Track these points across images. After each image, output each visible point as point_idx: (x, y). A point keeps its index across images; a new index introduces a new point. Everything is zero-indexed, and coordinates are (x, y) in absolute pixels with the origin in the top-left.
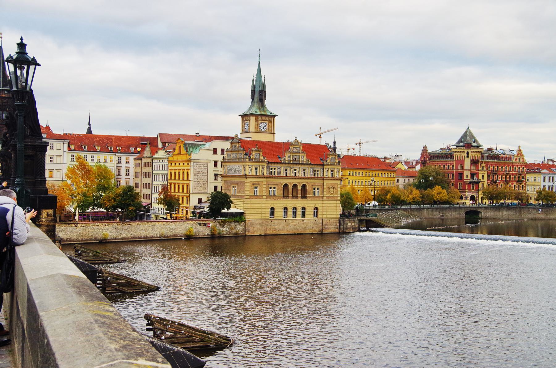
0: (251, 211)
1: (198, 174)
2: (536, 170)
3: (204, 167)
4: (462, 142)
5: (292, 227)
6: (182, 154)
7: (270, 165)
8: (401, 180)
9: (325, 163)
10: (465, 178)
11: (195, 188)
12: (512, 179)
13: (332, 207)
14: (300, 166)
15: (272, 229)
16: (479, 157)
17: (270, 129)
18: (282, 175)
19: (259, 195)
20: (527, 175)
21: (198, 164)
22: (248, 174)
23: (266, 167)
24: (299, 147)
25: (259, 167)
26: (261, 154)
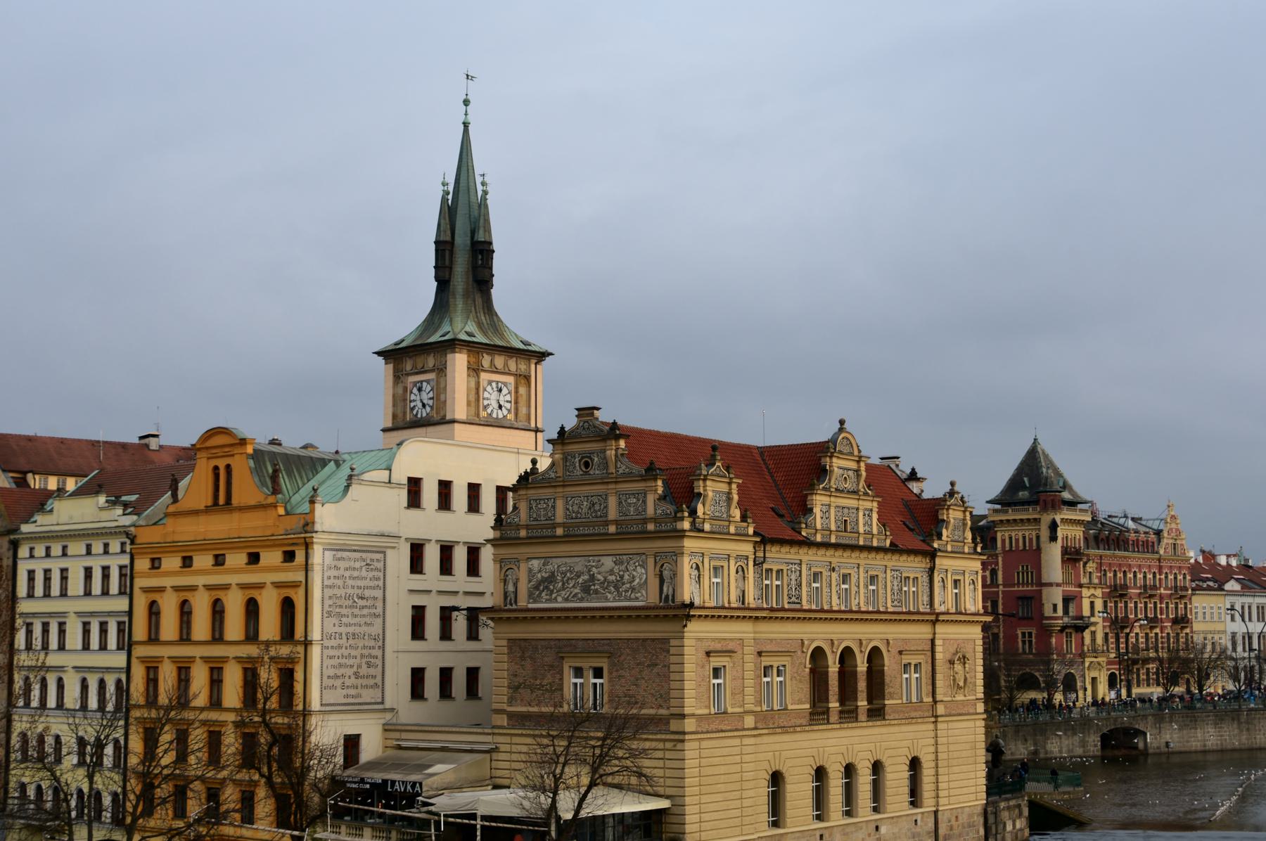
0: (705, 799)
1: (344, 611)
2: (1211, 584)
3: (371, 574)
4: (1024, 488)
6: (241, 509)
9: (936, 545)
10: (1048, 611)
11: (330, 682)
12: (1161, 614)
14: (863, 559)
16: (1079, 540)
17: (523, 410)
18: (806, 606)
20: (1194, 598)
21: (345, 554)
23: (751, 563)
26: (736, 497)
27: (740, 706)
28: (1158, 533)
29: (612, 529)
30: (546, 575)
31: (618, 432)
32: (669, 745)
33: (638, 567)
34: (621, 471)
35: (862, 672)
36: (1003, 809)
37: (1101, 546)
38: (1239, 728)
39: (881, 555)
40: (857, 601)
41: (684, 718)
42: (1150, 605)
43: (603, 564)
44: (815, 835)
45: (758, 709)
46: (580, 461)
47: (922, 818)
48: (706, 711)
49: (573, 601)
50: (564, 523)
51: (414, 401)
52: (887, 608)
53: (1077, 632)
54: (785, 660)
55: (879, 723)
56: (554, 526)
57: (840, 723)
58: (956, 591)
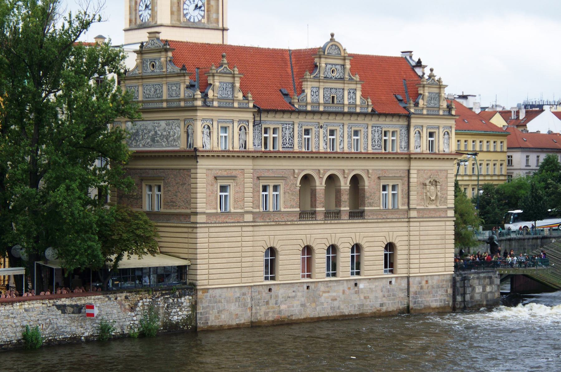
0: (211, 261)
5: (325, 305)
7: (264, 117)
8: (519, 158)
13: (434, 242)
14: (346, 120)
17: (214, 16)
18: (296, 149)
19: (233, 210)
22: (201, 149)
23: (251, 125)
24: (340, 62)
25: (231, 126)
26: (238, 85)
27: (242, 209)
30: (134, 131)
32: (190, 230)
33: (177, 127)
34: (169, 70)
35: (345, 190)
36: (473, 278)
40: (341, 147)
41: (197, 215)
43: (161, 125)
44: (303, 286)
45: (258, 210)
46: (150, 64)
48: (214, 211)
49: (147, 147)
50: (166, 100)
51: (141, 11)
55: (361, 221)
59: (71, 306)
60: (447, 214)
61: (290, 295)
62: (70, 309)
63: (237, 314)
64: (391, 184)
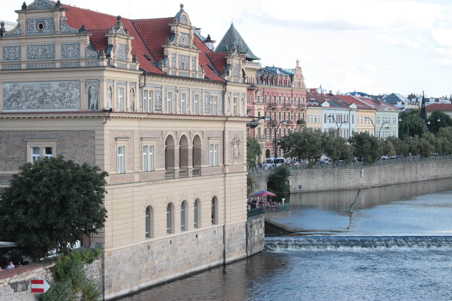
2: (315, 103)
5: (181, 258)
9: (226, 79)
12: (292, 119)
15: (149, 271)
20: (307, 110)
23: (138, 86)
25: (125, 87)
26: (131, 48)
28: (292, 76)
29: (58, 65)
31: (61, 7)
33: (75, 88)
34: (63, 30)
35: (190, 149)
37: (264, 82)
38: (334, 178)
39: (200, 84)
42: (287, 114)
44: (168, 241)
45: (141, 171)
46: (36, 24)
47: (218, 229)
48: (115, 173)
52: (203, 113)
53: (251, 128)
54: (153, 143)
56: (54, 62)
57: (180, 178)
58: (235, 104)
59: (21, 283)
60: (243, 169)
61: (160, 251)
62: (20, 287)
63: (130, 274)
64: (214, 144)
